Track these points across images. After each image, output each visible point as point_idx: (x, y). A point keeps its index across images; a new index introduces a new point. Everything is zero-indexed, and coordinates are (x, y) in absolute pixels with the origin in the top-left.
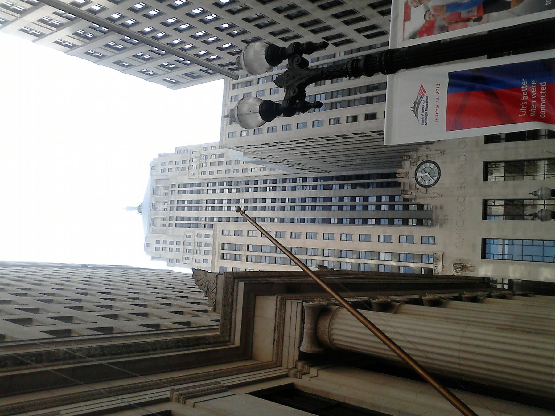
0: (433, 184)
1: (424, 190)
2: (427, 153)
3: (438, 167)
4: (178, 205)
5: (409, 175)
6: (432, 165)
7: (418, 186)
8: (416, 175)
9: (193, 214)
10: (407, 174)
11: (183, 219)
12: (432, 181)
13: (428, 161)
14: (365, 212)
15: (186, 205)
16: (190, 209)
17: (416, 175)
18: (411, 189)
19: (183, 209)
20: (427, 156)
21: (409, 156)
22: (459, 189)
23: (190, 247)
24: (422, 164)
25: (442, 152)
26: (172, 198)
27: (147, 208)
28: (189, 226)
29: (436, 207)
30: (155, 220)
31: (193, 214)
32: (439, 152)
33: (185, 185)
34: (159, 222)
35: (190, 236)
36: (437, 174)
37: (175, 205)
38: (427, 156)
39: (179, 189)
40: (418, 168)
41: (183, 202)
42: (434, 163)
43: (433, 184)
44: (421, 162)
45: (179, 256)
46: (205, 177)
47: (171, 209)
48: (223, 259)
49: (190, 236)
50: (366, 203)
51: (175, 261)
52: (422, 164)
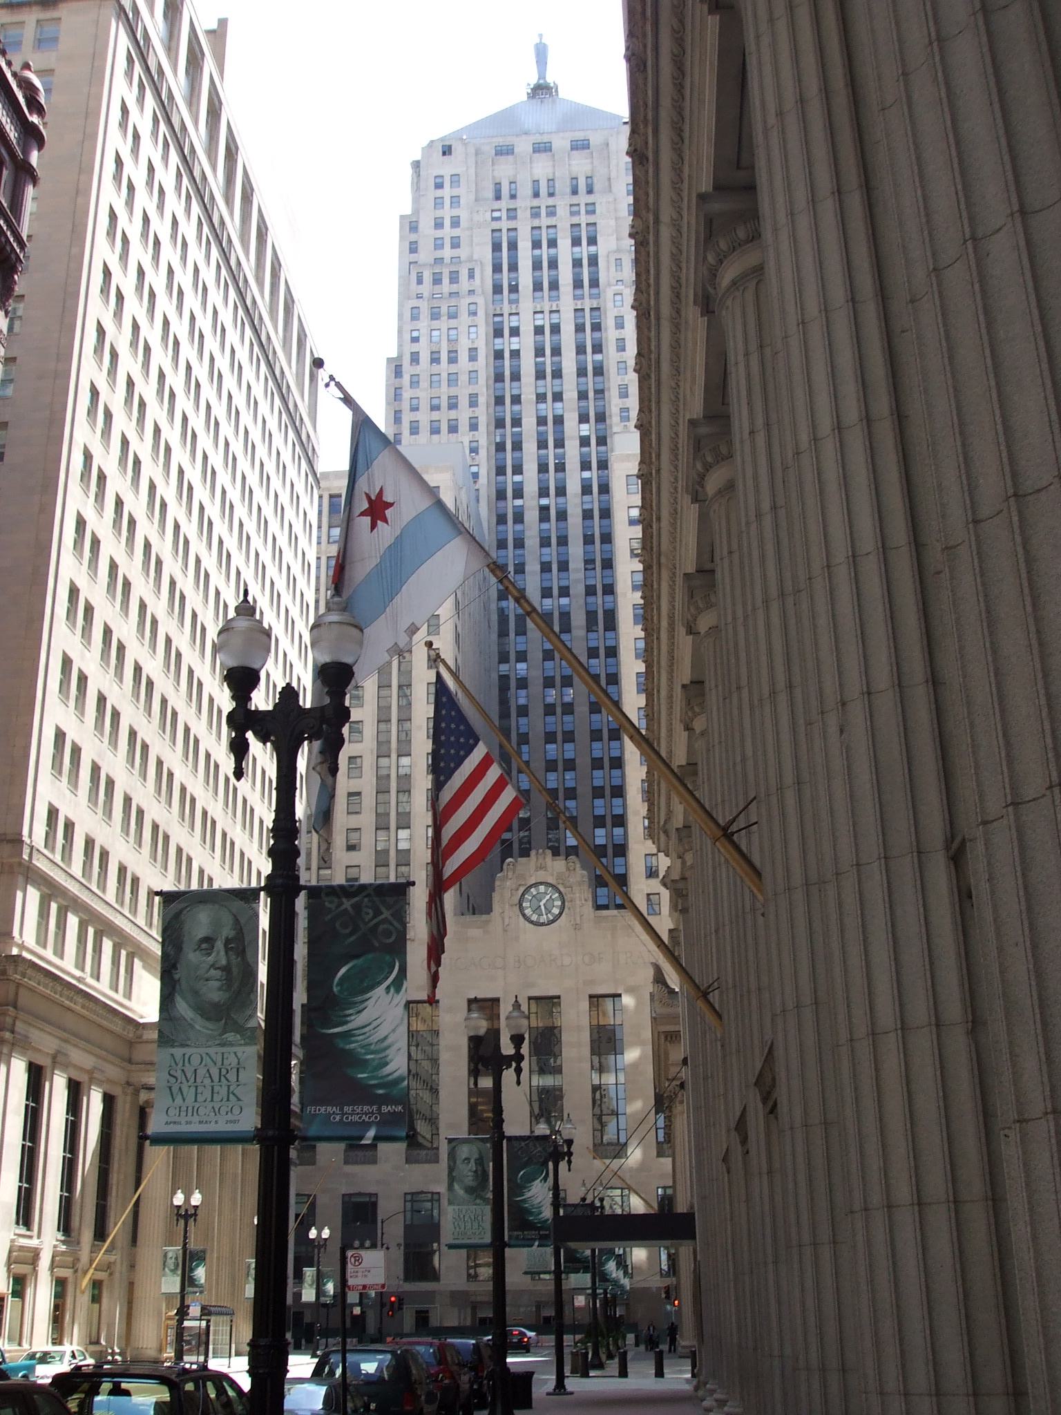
0: (524, 915)
1: (516, 899)
3: (553, 921)
4: (544, 230)
5: (542, 873)
6: (556, 911)
7: (522, 889)
8: (541, 883)
9: (525, 277)
11: (513, 246)
12: (528, 912)
13: (563, 903)
14: (541, 711)
15: (545, 252)
16: (537, 265)
17: (541, 883)
19: (536, 244)
23: (446, 280)
24: (560, 893)
25: (577, 927)
26: (562, 211)
27: (541, 119)
28: (497, 268)
30: (510, 157)
31: (525, 277)
33: (592, 241)
34: (504, 171)
35: (471, 275)
37: (544, 221)
39: (583, 226)
40: (552, 886)
41: (553, 243)
42: (561, 914)
43: (524, 915)
44: (562, 889)
45: (426, 254)
46: (610, 305)
47: (535, 213)
48: (417, 409)
49: (471, 275)
50: (559, 710)
51: (413, 237)
52: (560, 893)
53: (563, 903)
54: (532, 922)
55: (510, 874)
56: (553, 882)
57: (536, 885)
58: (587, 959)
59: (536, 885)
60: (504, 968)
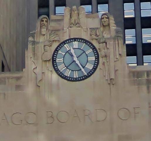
1: (49, 55)
2: (112, 56)
3: (86, 77)
5: (74, 28)
6: (90, 67)
7: (55, 45)
8: (75, 39)
10: (77, 24)
12: (61, 68)
13: (97, 58)
17: (75, 39)
18: (50, 35)
20: (106, 56)
21: (109, 25)
22: (50, 114)
25: (111, 82)
29: (18, 79)
32: (113, 77)
36: (76, 75)
38: (106, 56)
40: (86, 42)
42: (95, 69)
43: (57, 71)
52: (94, 48)
53: (97, 58)
54: (65, 78)
55: (44, 31)
56: (87, 38)
57: (71, 40)
58: (122, 114)
59: (71, 40)
60: (35, 124)
